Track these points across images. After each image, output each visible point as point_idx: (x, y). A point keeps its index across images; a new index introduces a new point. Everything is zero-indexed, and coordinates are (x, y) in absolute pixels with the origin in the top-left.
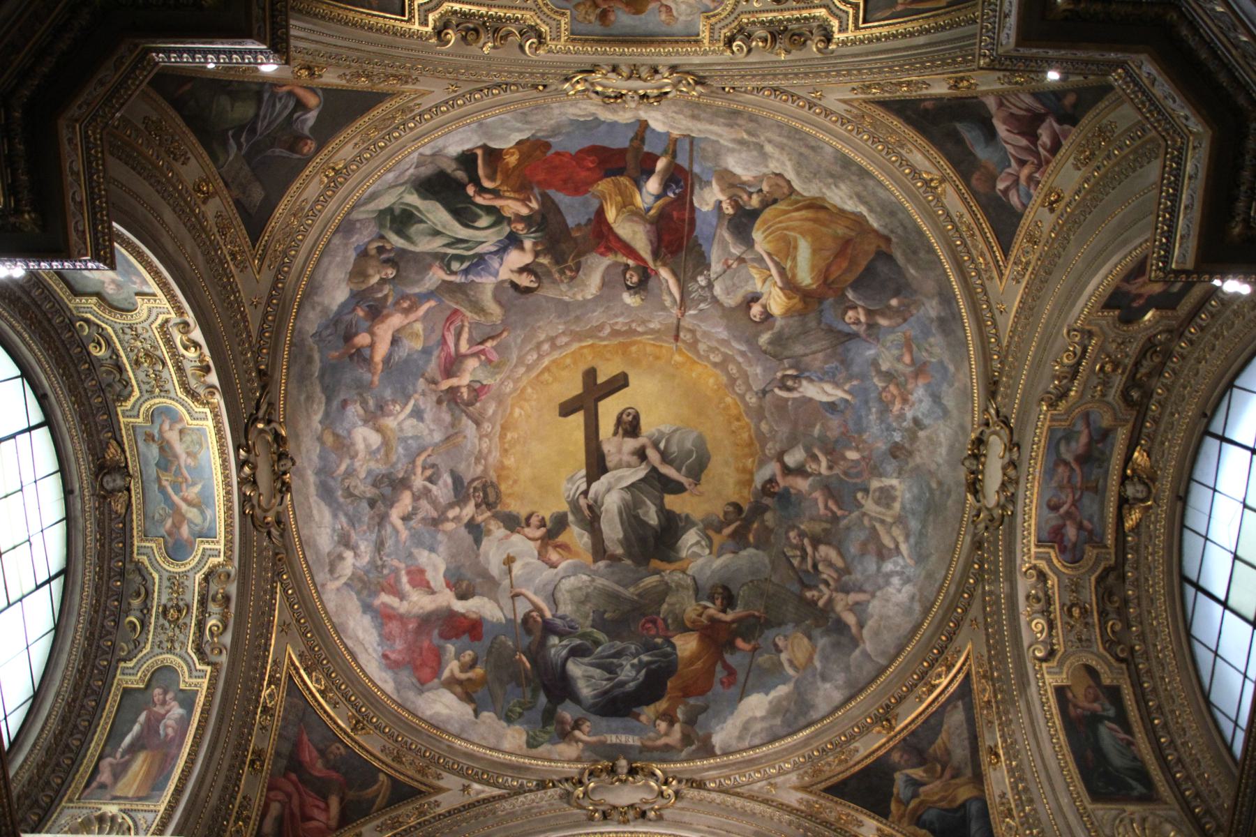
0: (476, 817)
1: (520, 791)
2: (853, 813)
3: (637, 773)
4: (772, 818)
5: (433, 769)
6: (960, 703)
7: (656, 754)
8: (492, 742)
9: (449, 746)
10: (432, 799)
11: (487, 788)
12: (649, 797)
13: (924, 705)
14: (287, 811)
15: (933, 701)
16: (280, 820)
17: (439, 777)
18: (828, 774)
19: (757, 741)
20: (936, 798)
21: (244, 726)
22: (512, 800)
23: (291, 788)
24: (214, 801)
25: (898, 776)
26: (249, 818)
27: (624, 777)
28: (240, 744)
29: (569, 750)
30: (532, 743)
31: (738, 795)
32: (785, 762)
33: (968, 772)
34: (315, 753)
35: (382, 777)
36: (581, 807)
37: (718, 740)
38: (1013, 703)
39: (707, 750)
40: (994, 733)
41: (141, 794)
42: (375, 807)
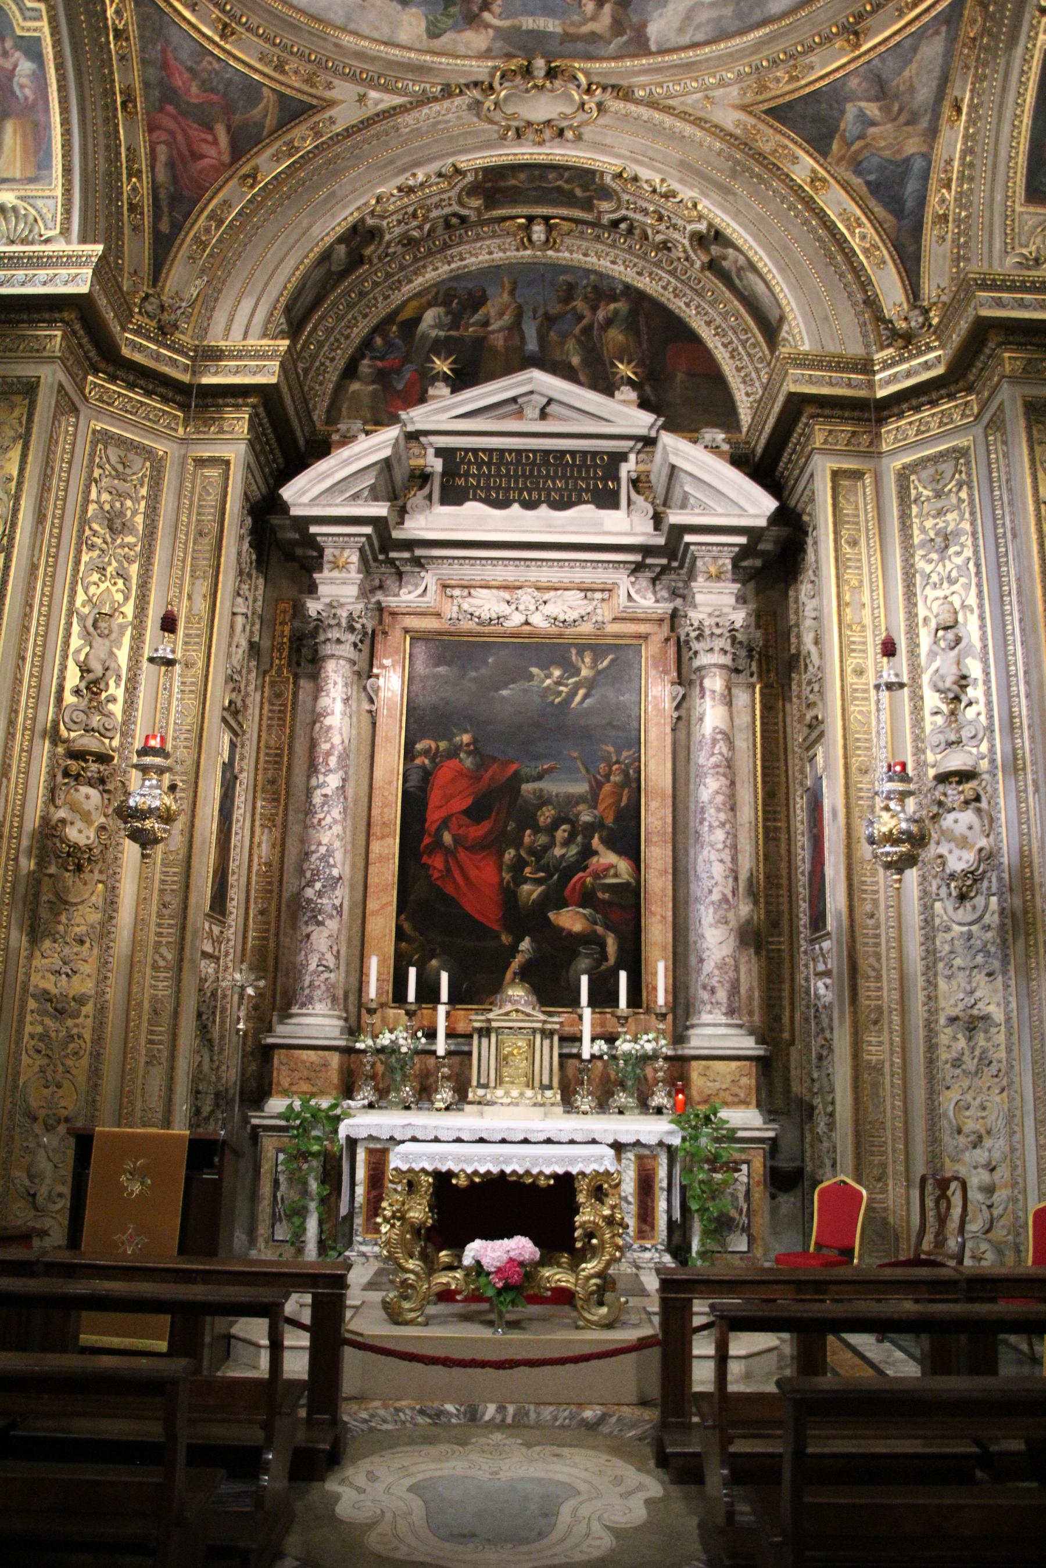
0: (377, 136)
1: (425, 100)
2: (791, 146)
3: (555, 77)
4: (701, 145)
5: (323, 77)
6: (944, 29)
7: (580, 46)
8: (385, 33)
9: (336, 45)
10: (327, 115)
11: (386, 96)
12: (568, 111)
13: (902, 23)
14: (175, 152)
15: (917, 17)
16: (171, 165)
17: (329, 86)
18: (773, 93)
19: (700, 37)
20: (883, 144)
21: (102, 67)
22: (415, 114)
23: (171, 125)
24: (102, 166)
25: (851, 110)
26: (141, 171)
27: (540, 82)
28: (105, 90)
29: (477, 40)
30: (434, 32)
31: (668, 110)
32: (728, 71)
33: (924, 123)
34: (187, 75)
35: (265, 90)
36: (491, 121)
37: (654, 30)
38: (996, 56)
39: (640, 46)
40: (966, 82)
41: (29, 175)
42: (265, 133)
